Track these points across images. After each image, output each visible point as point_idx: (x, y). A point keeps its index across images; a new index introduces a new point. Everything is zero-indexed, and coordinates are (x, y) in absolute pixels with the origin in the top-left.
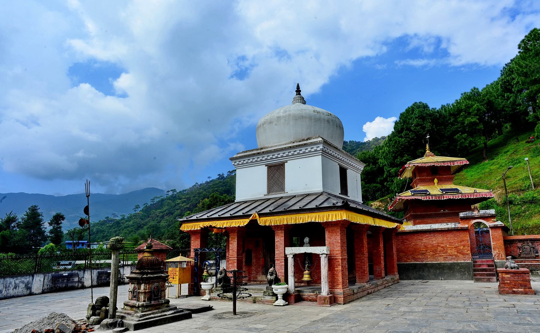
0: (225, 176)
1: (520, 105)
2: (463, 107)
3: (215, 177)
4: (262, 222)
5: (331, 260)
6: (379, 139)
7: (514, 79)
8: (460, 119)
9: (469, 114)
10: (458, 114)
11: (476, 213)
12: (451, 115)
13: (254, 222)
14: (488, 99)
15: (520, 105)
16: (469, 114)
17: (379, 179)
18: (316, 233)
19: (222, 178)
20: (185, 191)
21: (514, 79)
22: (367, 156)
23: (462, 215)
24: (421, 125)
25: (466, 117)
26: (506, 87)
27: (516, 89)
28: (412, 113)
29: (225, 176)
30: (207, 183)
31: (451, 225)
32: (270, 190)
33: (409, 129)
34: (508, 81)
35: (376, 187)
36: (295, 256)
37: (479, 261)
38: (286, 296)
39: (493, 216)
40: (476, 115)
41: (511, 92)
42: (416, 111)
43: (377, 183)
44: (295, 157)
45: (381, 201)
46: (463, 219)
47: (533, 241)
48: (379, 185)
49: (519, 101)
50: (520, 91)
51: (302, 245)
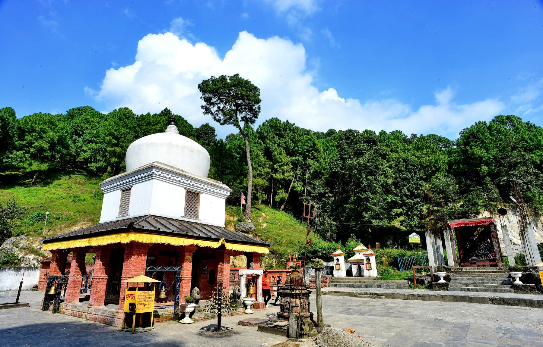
1: (85, 151)
2: (38, 128)
4: (229, 246)
7: (87, 128)
9: (41, 137)
12: (19, 128)
13: (223, 246)
14: (63, 133)
16: (41, 137)
21: (87, 128)
26: (76, 131)
27: (88, 138)
34: (82, 127)
40: (48, 142)
49: (84, 148)
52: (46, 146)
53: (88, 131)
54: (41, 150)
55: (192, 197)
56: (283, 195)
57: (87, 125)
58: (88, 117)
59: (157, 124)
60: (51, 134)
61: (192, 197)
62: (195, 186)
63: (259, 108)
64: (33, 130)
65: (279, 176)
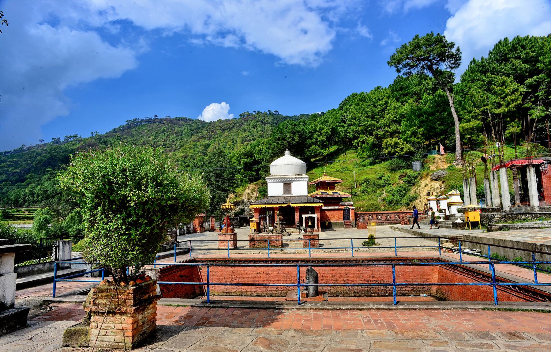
0: (61, 141)
1: (349, 133)
2: (318, 129)
3: (49, 140)
4: (292, 205)
5: (318, 218)
6: (223, 121)
8: (315, 136)
9: (321, 133)
10: (315, 133)
11: (346, 203)
12: (309, 132)
15: (349, 133)
17: (254, 169)
18: (312, 210)
19: (57, 143)
20: (8, 152)
22: (247, 151)
23: (341, 203)
24: (293, 138)
25: (319, 136)
27: (349, 122)
28: (286, 128)
29: (61, 141)
30: (38, 146)
31: (337, 208)
32: (284, 193)
33: (284, 139)
35: (251, 174)
36: (306, 218)
37: (346, 221)
38: (304, 230)
39: (352, 205)
40: (325, 135)
41: (345, 123)
42: (290, 129)
43: (253, 171)
44: (296, 181)
45: (255, 185)
46: (342, 205)
47: (363, 214)
48: (254, 173)
50: (350, 125)
51: (308, 214)
52: (324, 138)
53: (348, 117)
54: (323, 141)
55: (287, 186)
56: (514, 128)
57: (348, 114)
58: (348, 106)
59: (383, 99)
60: (326, 129)
61: (287, 186)
62: (287, 181)
63: (458, 50)
64: (316, 131)
65: (500, 111)
